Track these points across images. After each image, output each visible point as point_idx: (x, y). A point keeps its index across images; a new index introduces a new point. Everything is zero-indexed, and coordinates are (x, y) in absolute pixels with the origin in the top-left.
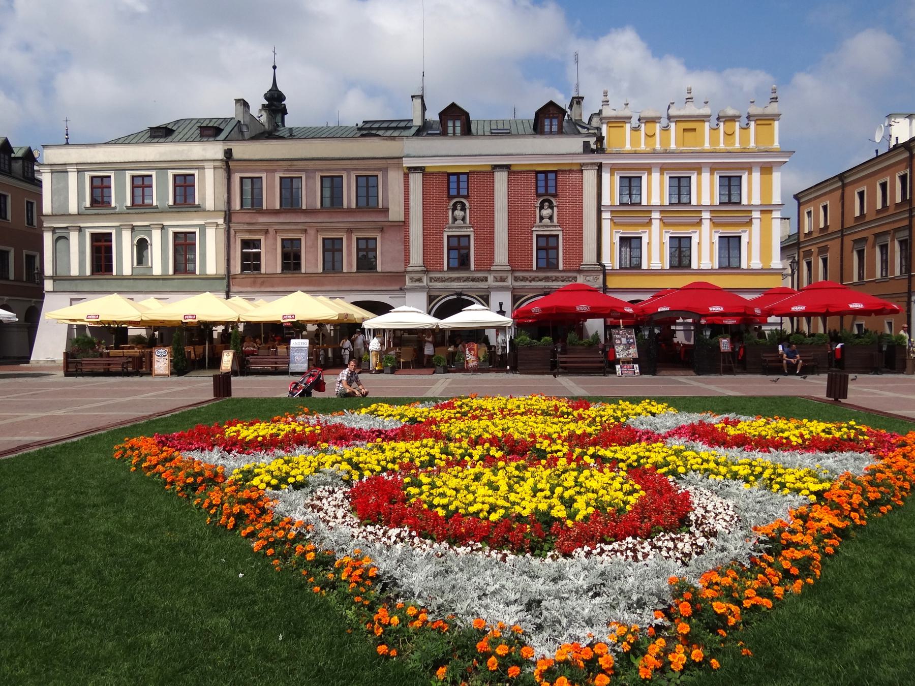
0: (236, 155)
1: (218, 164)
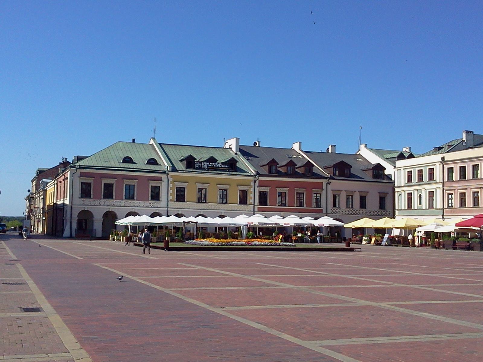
1: (440, 163)
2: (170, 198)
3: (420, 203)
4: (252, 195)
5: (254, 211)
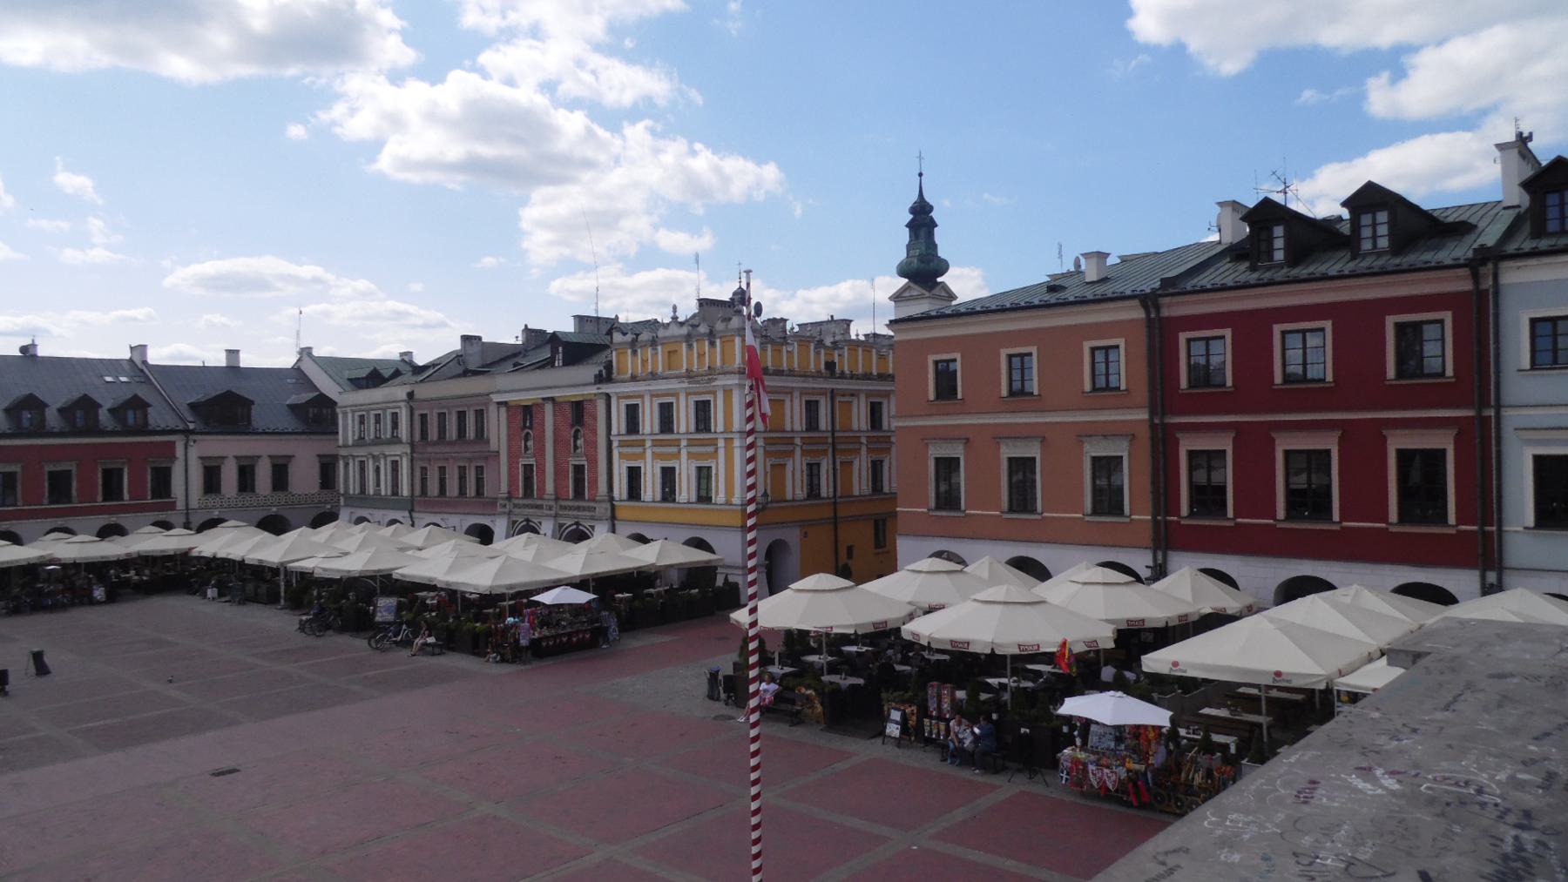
0: (417, 395)
3: (378, 484)
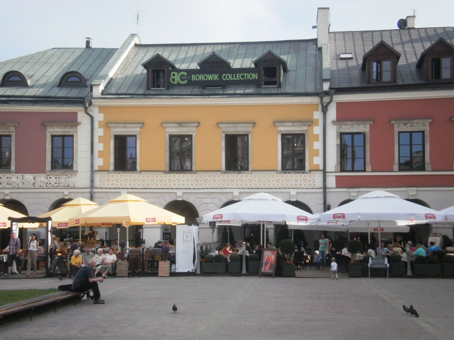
2: (99, 162)
4: (318, 145)
5: (325, 188)
